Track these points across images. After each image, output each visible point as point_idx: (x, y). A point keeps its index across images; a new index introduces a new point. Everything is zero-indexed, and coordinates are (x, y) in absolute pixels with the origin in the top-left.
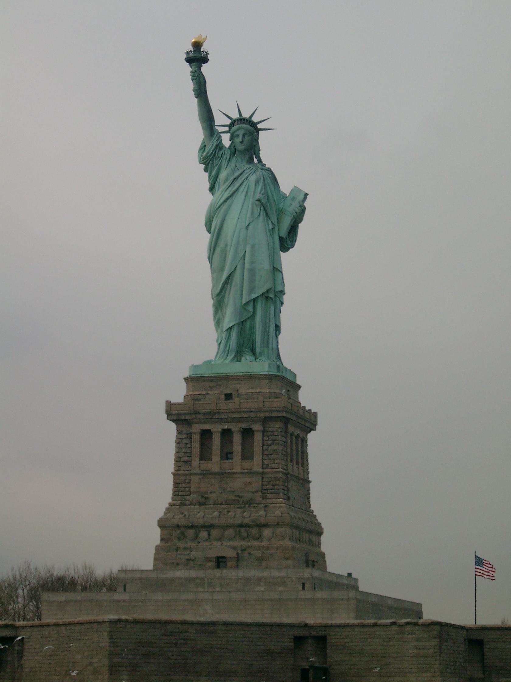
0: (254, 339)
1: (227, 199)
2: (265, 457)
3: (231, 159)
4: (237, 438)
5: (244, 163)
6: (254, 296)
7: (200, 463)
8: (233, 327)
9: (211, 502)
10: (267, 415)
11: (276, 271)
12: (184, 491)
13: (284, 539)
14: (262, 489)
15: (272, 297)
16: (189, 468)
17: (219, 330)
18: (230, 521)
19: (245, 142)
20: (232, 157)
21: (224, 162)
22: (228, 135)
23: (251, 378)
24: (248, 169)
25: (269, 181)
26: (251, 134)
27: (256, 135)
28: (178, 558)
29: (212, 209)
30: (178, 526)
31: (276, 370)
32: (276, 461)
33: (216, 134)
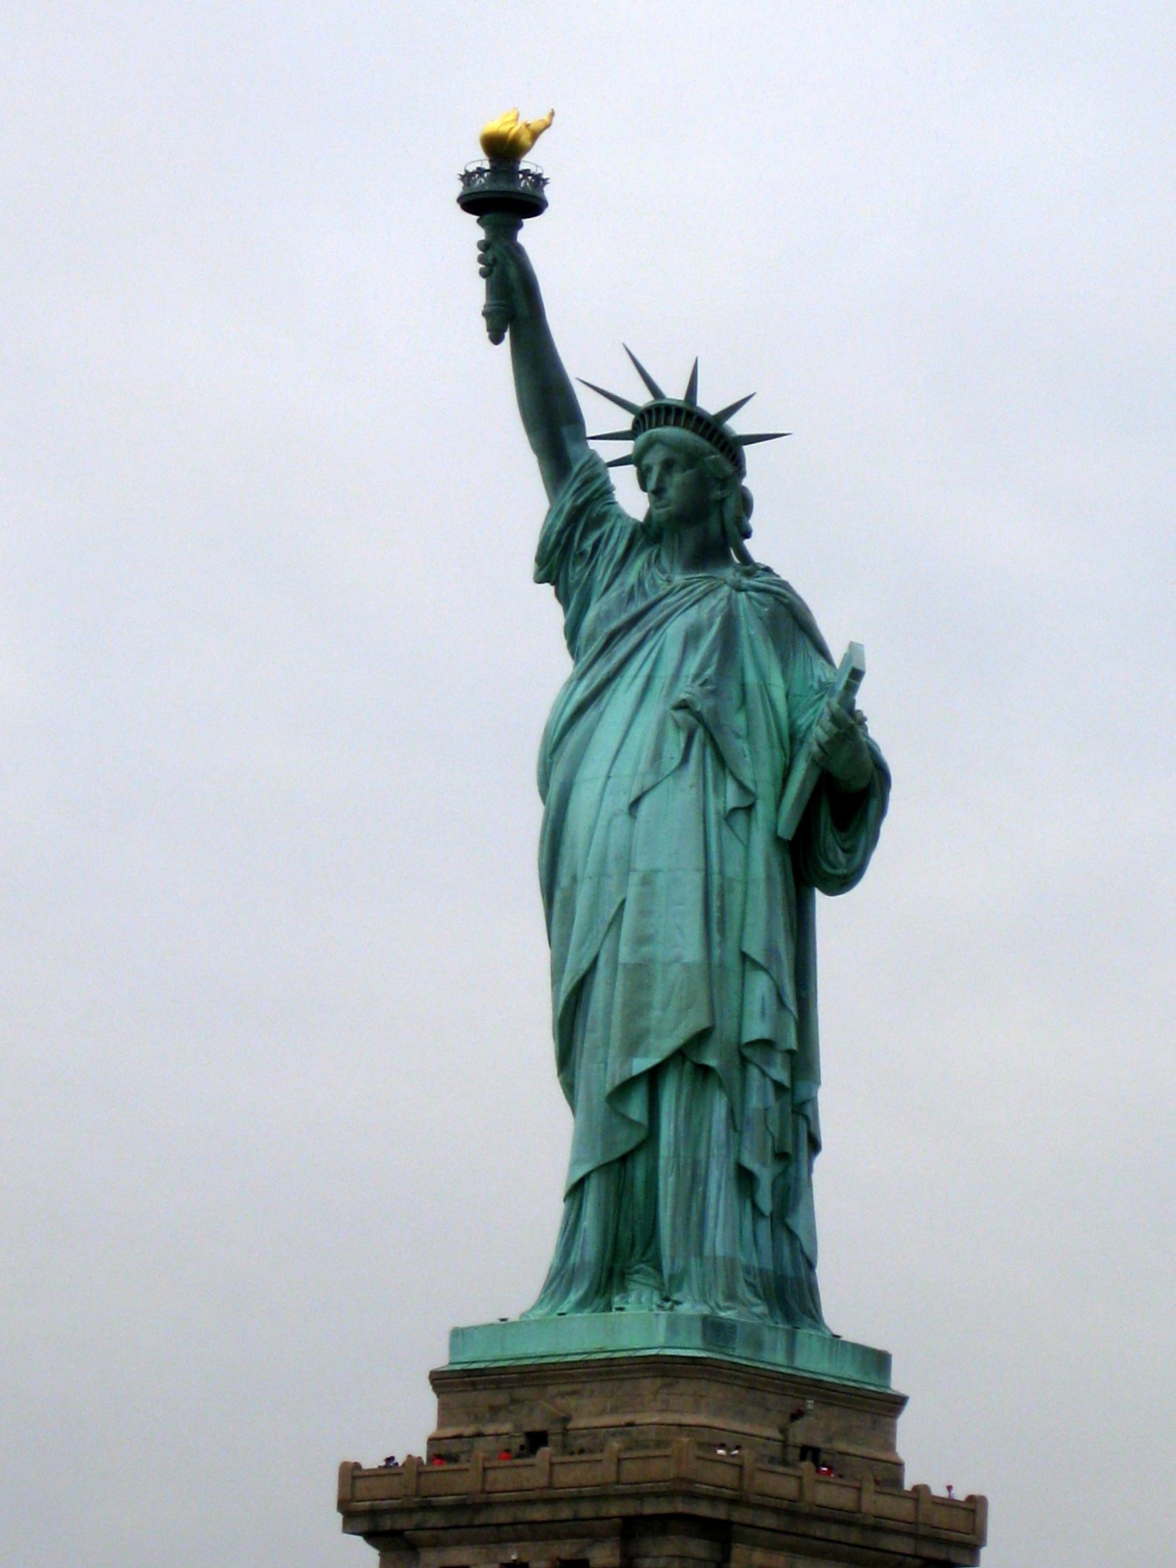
3: (630, 560)
5: (678, 570)
6: (641, 1064)
10: (630, 1508)
11: (748, 965)
15: (711, 1061)
19: (672, 493)
20: (638, 554)
21: (602, 572)
22: (631, 471)
23: (608, 1373)
24: (676, 590)
25: (752, 632)
26: (693, 458)
27: (715, 462)
31: (698, 1341)
33: (576, 468)
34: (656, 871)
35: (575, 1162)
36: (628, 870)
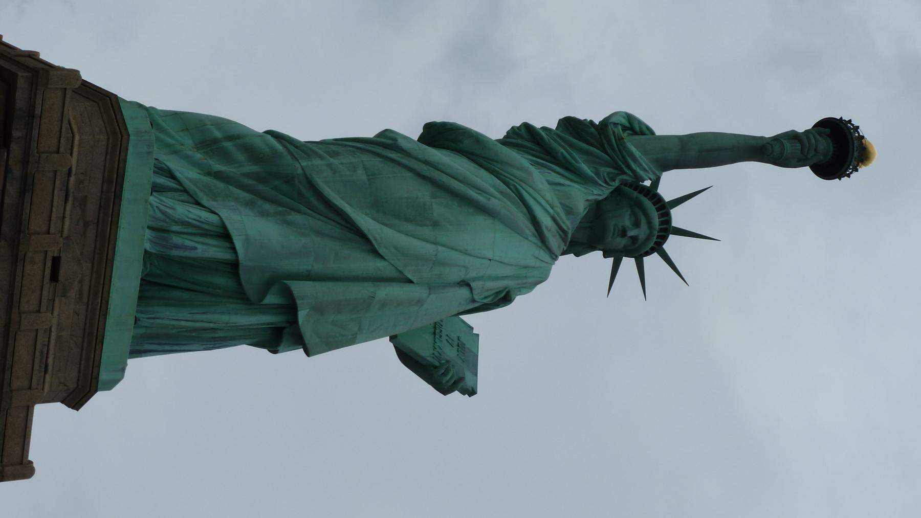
0: (177, 294)
1: (536, 223)
6: (302, 315)
8: (228, 245)
17: (189, 142)
34: (421, 306)
35: (247, 241)
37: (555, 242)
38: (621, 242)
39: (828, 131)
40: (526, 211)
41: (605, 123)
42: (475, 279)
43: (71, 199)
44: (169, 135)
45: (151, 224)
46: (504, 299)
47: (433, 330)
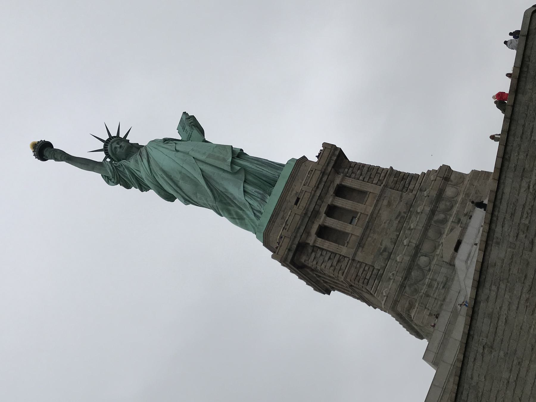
0: (264, 179)
1: (149, 162)
2: (370, 180)
4: (340, 202)
6: (230, 160)
7: (347, 246)
8: (245, 189)
9: (390, 246)
12: (367, 273)
13: (464, 178)
14: (402, 191)
16: (347, 259)
18: (420, 227)
23: (293, 178)
28: (437, 297)
29: (150, 179)
30: (402, 286)
32: (379, 171)
35: (239, 188)
36: (188, 154)
37: (144, 153)
38: (122, 144)
39: (44, 157)
40: (151, 167)
41: (117, 184)
42: (173, 151)
43: (286, 221)
44: (252, 225)
45: (265, 203)
46: (166, 140)
47: (191, 137)
